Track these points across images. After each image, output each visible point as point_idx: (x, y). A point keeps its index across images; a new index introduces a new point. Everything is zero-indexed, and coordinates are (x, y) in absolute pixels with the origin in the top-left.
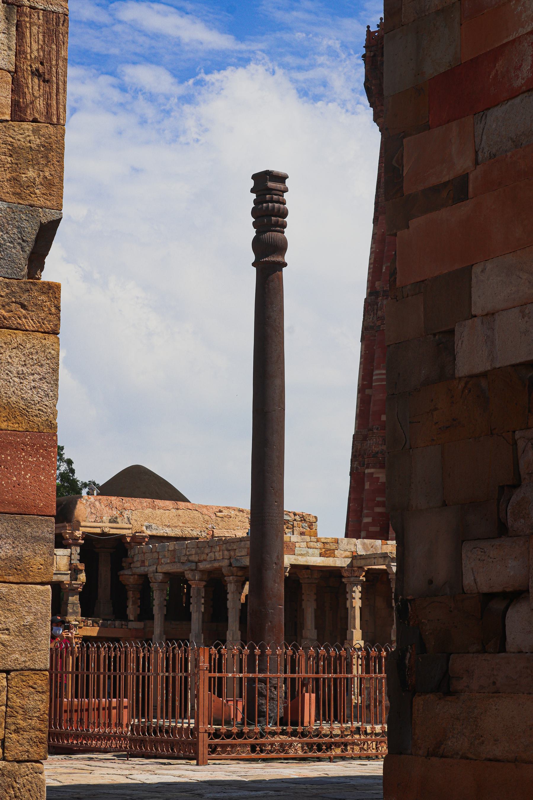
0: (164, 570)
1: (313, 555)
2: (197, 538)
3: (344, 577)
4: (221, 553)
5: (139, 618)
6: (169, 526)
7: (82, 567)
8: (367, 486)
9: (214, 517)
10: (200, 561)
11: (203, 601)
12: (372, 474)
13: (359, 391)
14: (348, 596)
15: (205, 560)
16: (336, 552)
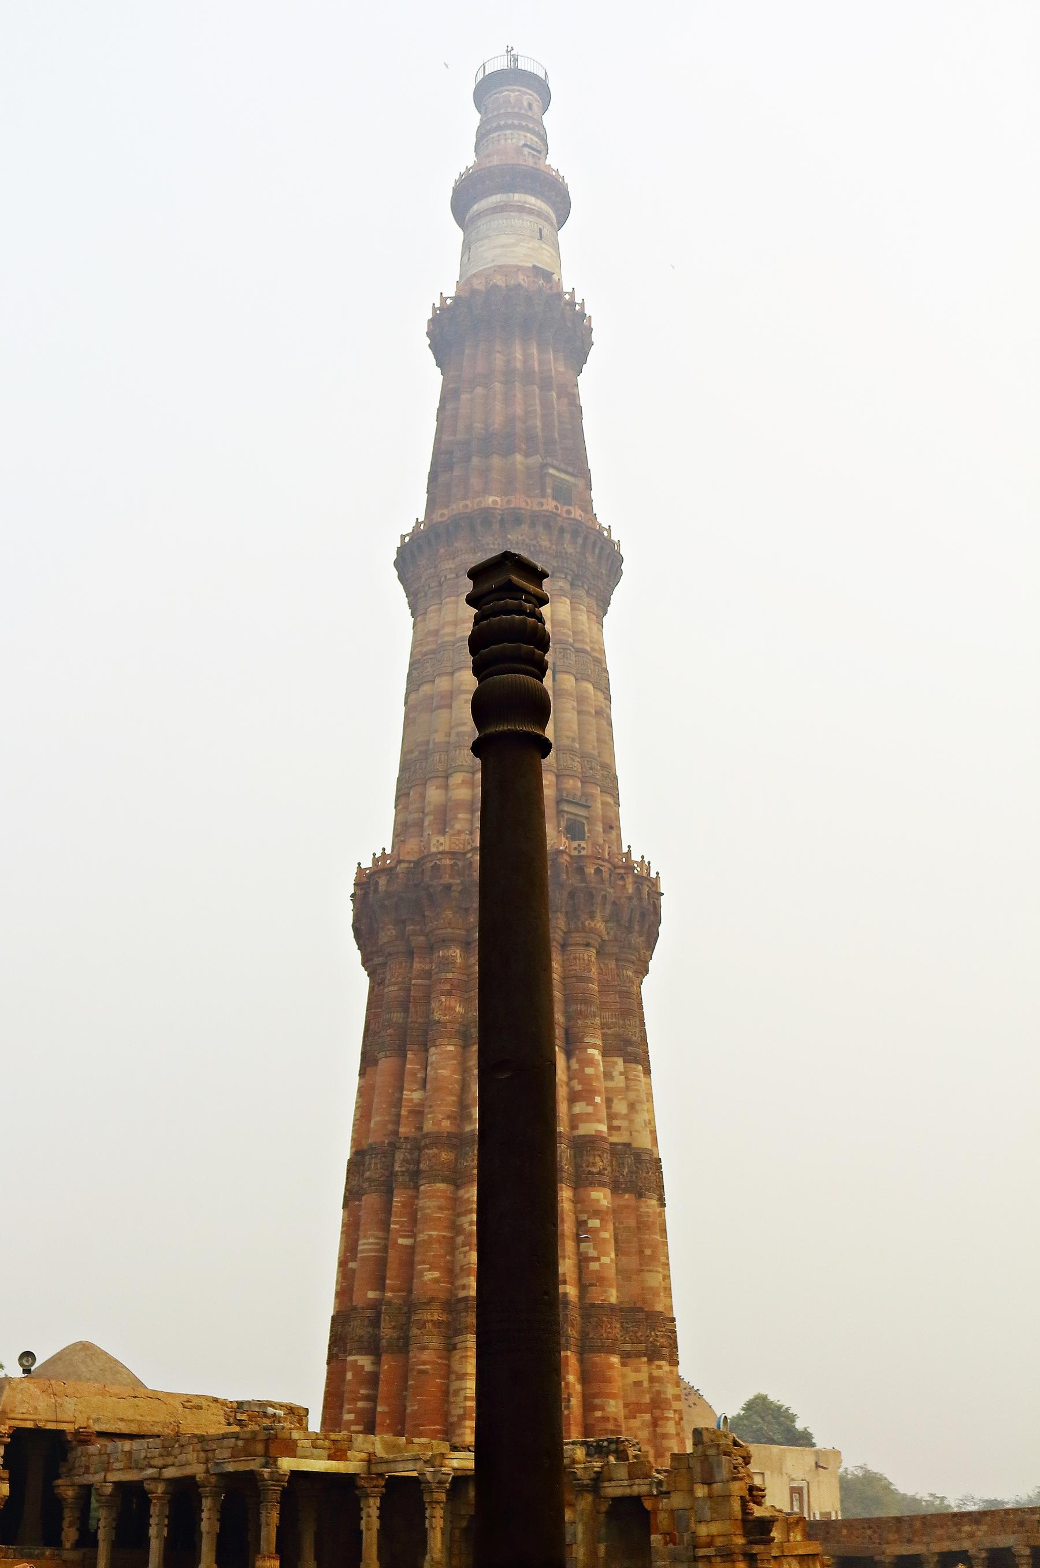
0: (116, 1479)
1: (319, 1458)
2: (159, 1436)
3: (357, 1488)
4: (195, 1455)
5: (77, 1545)
6: (122, 1420)
7: (6, 1474)
8: (349, 1376)
9: (181, 1408)
10: (165, 1467)
11: (166, 1522)
12: (356, 1361)
13: (343, 1264)
14: (364, 1514)
15: (173, 1465)
16: (349, 1453)
